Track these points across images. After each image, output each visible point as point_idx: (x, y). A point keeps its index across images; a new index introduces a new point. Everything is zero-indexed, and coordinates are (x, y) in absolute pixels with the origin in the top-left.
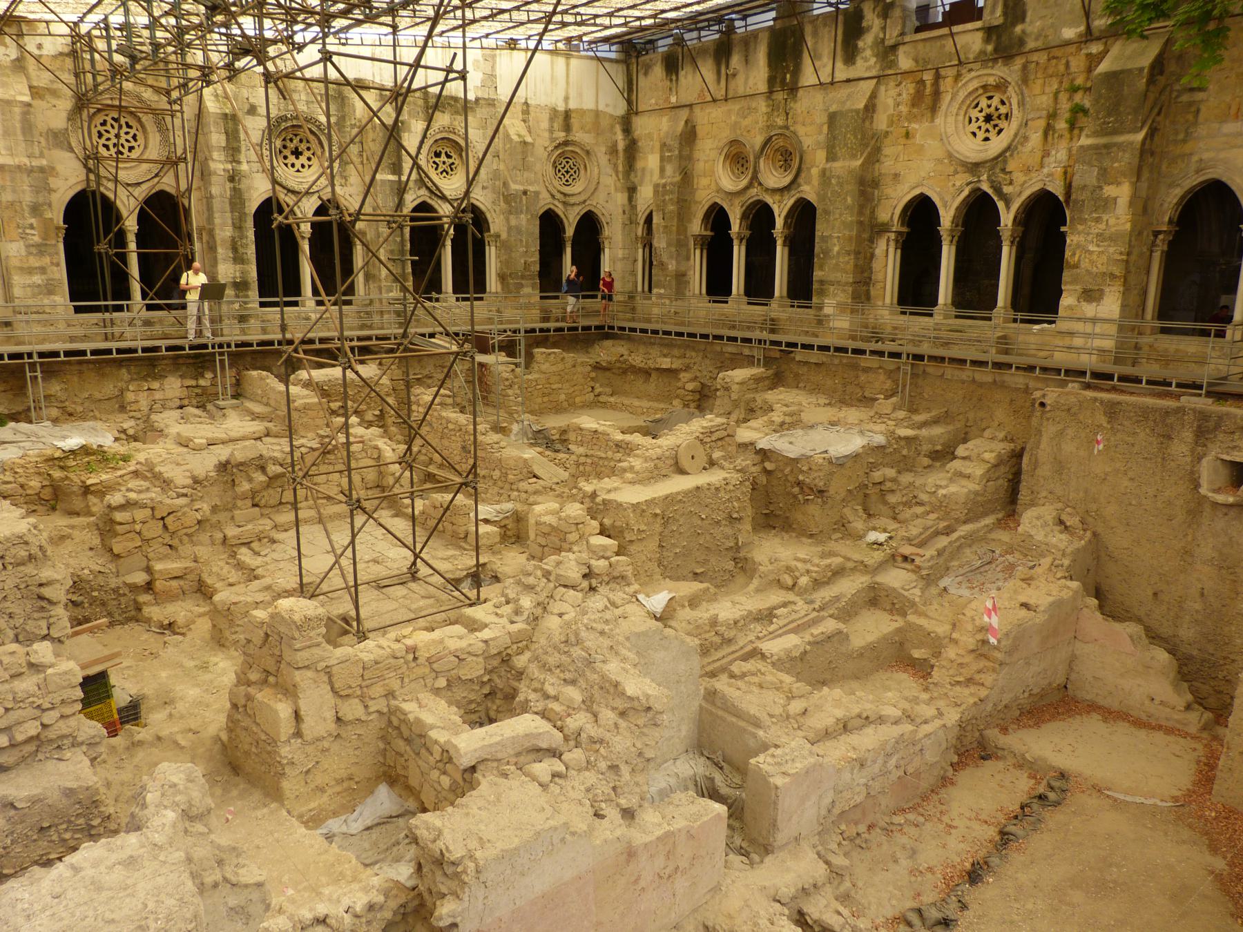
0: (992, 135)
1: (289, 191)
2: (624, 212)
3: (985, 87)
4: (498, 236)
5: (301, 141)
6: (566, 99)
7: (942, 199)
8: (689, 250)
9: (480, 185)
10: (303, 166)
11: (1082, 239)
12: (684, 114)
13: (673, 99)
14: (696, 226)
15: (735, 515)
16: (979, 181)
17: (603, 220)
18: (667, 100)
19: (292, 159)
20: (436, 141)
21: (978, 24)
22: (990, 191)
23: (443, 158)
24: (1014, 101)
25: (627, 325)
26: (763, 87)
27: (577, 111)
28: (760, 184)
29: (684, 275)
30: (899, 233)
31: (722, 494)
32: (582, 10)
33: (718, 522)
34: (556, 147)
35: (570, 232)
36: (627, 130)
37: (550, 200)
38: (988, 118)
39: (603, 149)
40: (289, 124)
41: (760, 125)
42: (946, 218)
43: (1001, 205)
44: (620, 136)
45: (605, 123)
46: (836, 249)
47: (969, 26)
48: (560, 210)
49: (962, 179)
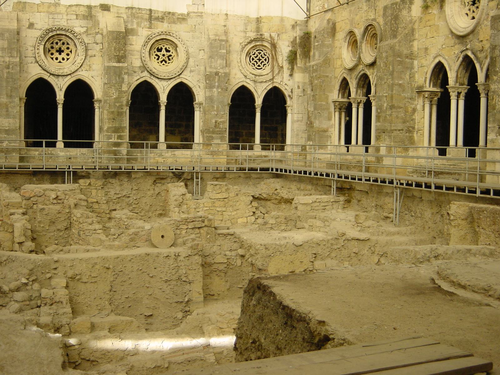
1: (51, 74)
2: (299, 87)
4: (200, 104)
5: (63, 44)
7: (449, 64)
8: (330, 113)
9: (188, 69)
10: (63, 59)
11: (496, 87)
12: (329, 15)
14: (335, 95)
15: (184, 279)
16: (467, 49)
17: (286, 93)
18: (323, 7)
19: (56, 55)
20: (157, 41)
22: (472, 56)
23: (164, 52)
25: (303, 169)
27: (266, 17)
29: (325, 131)
30: (432, 92)
31: (171, 261)
33: (166, 281)
34: (249, 43)
35: (259, 102)
37: (244, 79)
39: (287, 43)
40: (55, 33)
41: (363, 20)
43: (477, 66)
45: (288, 26)
46: (385, 105)
48: (251, 86)
49: (458, 49)
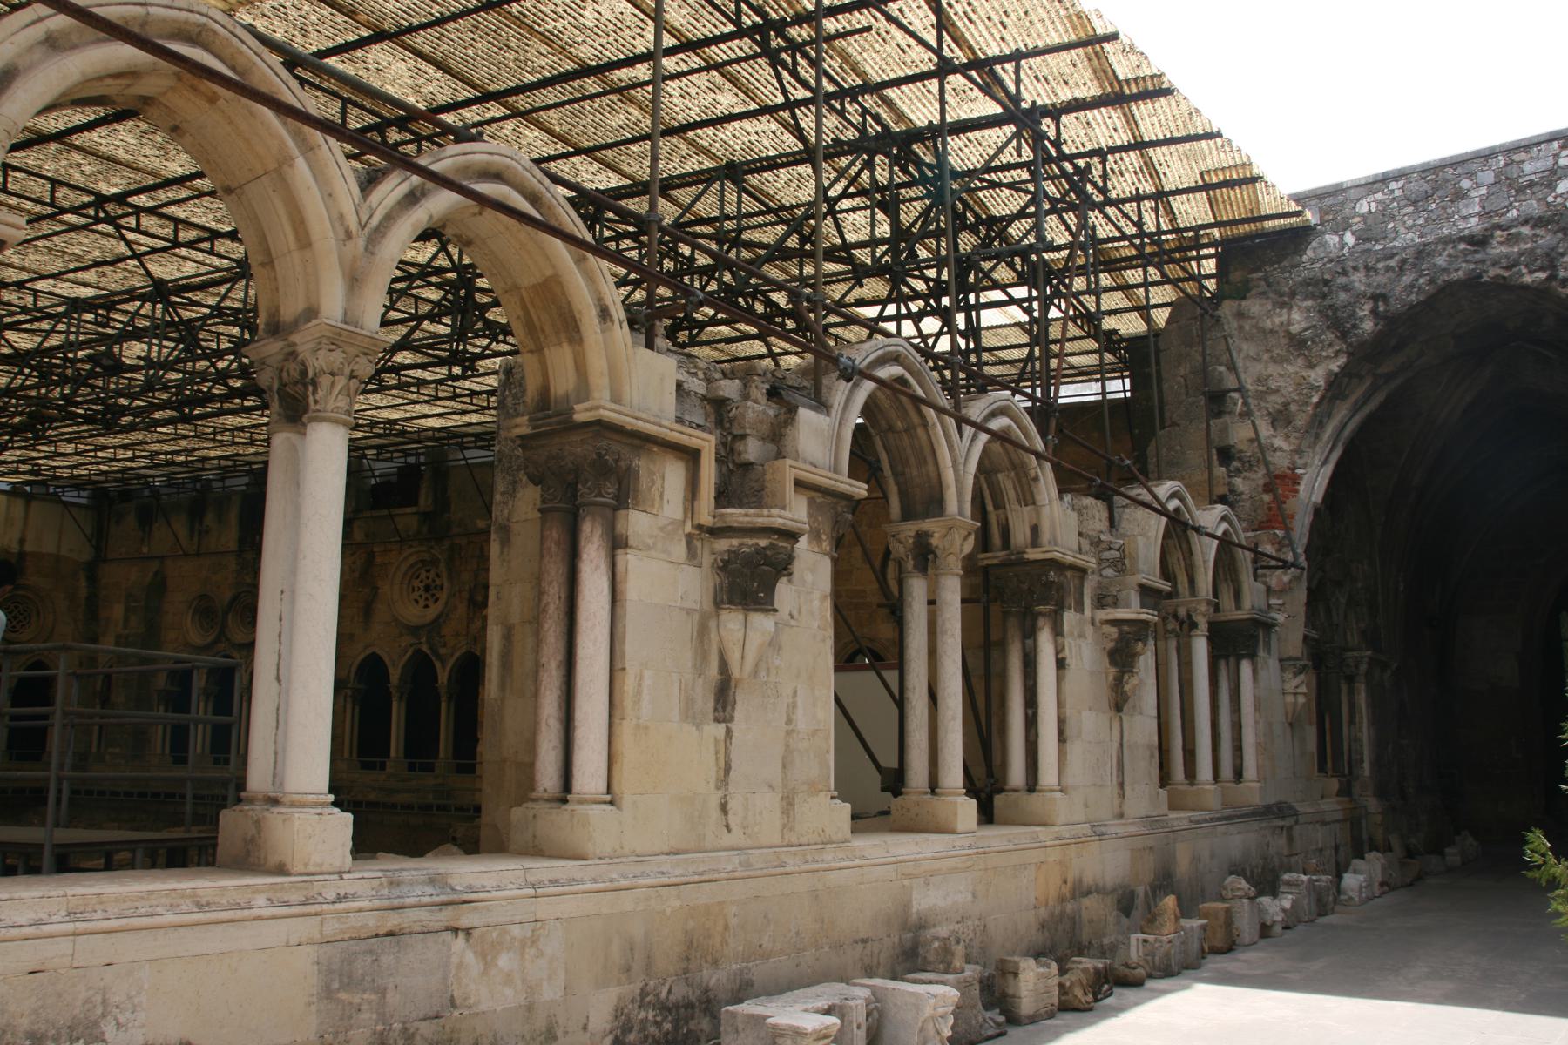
0: (430, 603)
3: (423, 561)
6: (22, 541)
13: (145, 550)
21: (414, 509)
22: (428, 652)
24: (445, 574)
26: (233, 546)
28: (228, 639)
32: (41, 462)
36: (93, 579)
38: (427, 589)
42: (395, 675)
43: (438, 664)
44: (83, 583)
47: (408, 510)
49: (406, 640)
